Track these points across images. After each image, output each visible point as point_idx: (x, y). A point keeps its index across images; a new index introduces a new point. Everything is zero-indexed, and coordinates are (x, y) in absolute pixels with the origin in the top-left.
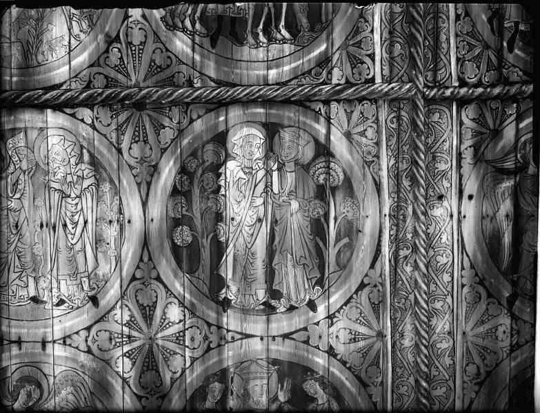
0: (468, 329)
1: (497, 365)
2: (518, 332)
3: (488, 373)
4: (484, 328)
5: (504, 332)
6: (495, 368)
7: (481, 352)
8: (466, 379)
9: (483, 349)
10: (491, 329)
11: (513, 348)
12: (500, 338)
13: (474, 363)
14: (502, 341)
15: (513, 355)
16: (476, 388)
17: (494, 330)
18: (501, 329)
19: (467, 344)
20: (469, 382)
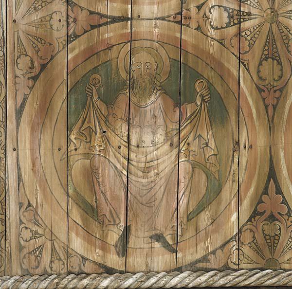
0: (17, 16)
1: (52, 58)
2: (75, 21)
3: (43, 67)
4: (37, 16)
5: (60, 21)
6: (51, 59)
7: (34, 43)
8: (18, 73)
9: (37, 40)
10: (45, 17)
11: (69, 39)
12: (55, 27)
13: (27, 55)
14: (58, 30)
15: (69, 46)
16: (31, 82)
17: (48, 18)
18: (56, 17)
19: (18, 33)
20: (22, 77)
